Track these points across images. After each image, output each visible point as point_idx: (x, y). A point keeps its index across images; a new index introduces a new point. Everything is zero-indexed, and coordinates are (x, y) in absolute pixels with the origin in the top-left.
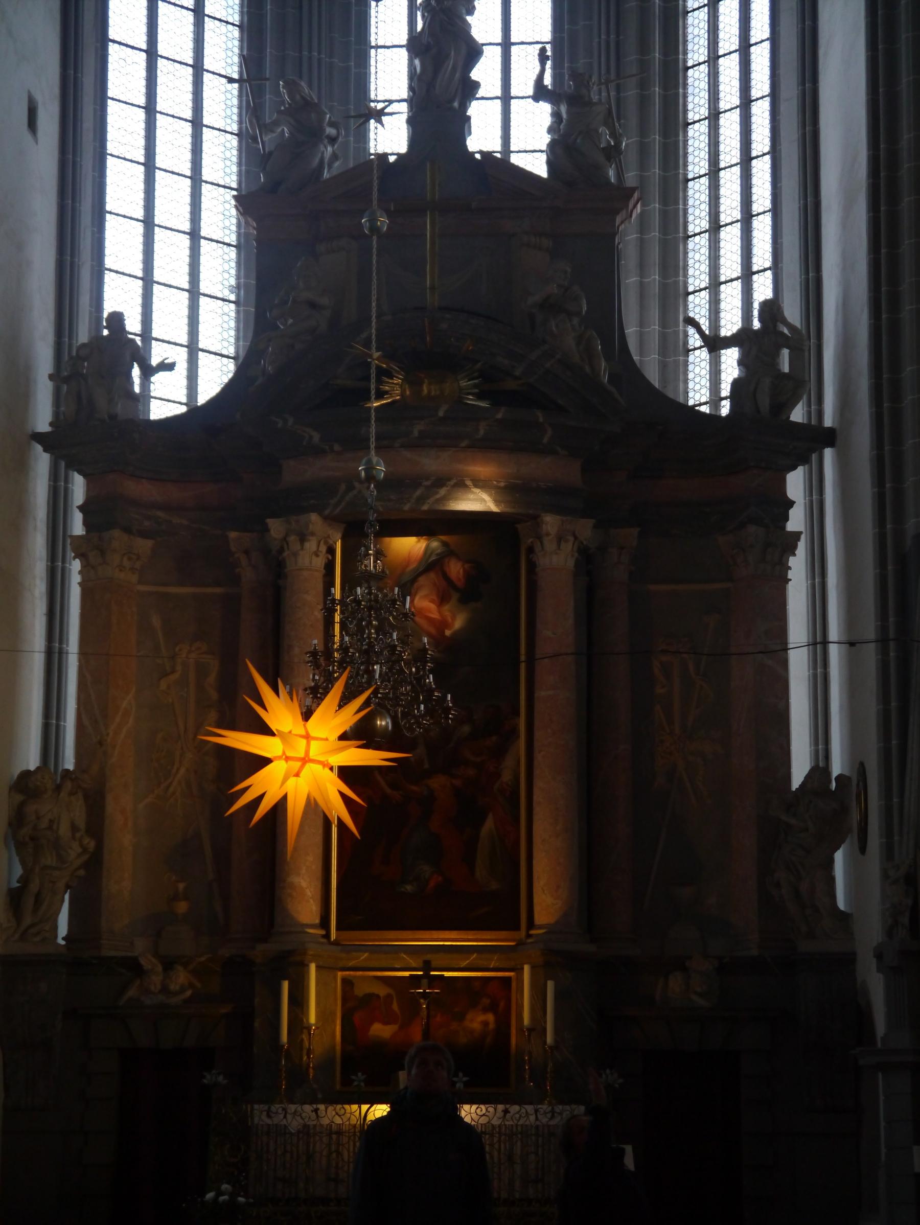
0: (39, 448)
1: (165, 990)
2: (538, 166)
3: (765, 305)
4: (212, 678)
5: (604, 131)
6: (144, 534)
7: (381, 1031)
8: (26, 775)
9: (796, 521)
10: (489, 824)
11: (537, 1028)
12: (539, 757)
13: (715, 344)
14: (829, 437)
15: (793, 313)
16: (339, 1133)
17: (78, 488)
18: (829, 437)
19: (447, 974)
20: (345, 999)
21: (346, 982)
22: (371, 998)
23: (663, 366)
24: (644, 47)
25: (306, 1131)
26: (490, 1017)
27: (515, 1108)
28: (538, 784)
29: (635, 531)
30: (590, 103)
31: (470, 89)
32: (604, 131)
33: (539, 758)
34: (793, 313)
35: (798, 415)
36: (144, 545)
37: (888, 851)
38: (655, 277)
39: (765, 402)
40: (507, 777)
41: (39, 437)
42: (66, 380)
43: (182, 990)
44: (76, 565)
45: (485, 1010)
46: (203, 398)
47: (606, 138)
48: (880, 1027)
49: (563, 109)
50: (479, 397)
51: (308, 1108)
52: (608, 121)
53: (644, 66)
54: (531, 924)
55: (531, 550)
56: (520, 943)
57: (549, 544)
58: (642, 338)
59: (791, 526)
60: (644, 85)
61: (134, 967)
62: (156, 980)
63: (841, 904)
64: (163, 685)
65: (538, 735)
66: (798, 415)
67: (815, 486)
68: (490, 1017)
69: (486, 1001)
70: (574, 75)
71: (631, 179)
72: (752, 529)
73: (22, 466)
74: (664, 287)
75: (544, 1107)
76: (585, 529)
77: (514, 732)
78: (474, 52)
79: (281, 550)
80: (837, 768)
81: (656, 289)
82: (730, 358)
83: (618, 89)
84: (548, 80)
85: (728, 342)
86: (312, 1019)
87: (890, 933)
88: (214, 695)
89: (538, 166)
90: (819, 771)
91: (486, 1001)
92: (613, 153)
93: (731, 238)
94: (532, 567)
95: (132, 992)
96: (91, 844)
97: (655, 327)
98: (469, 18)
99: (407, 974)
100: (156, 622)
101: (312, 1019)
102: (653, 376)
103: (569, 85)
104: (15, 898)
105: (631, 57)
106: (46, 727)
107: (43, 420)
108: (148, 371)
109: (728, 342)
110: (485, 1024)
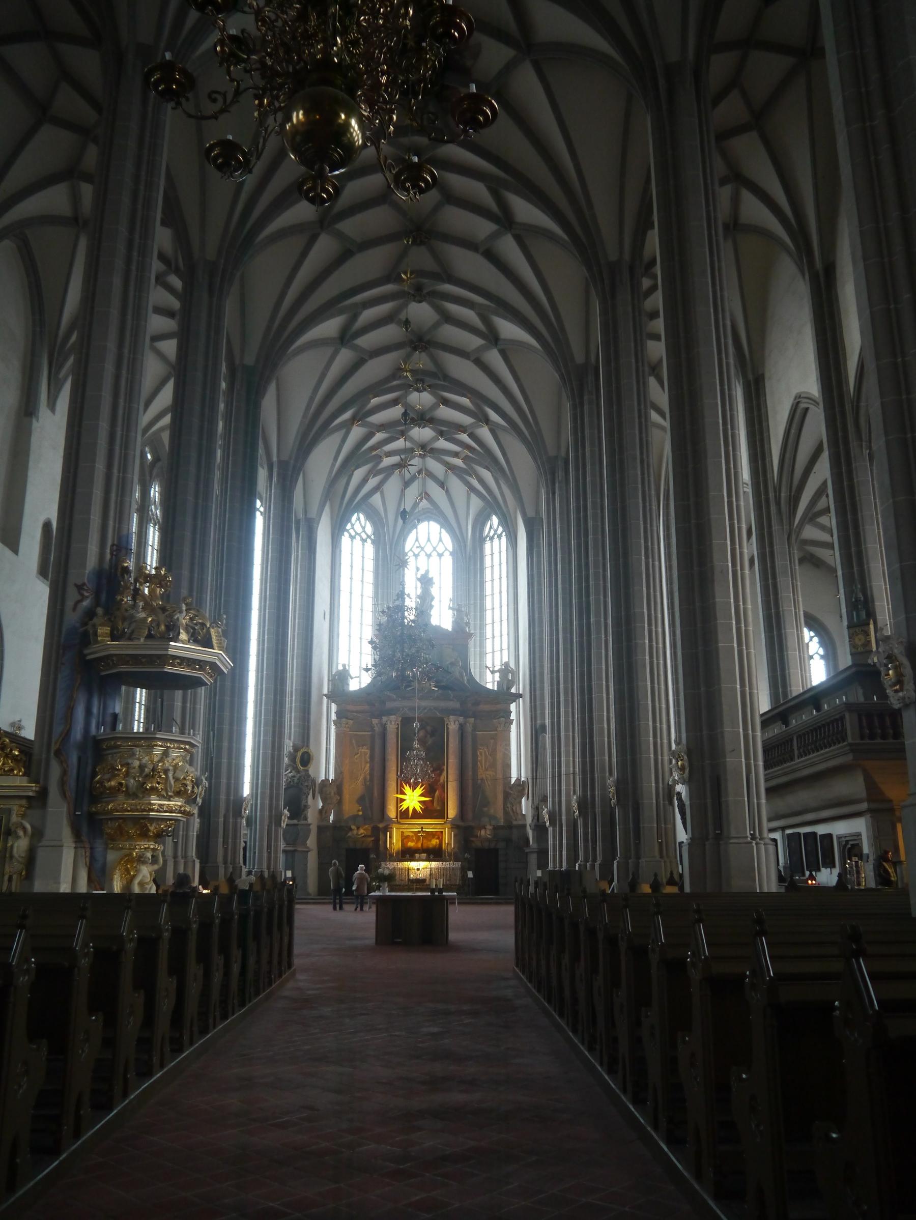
0: (325, 698)
1: (357, 834)
2: (450, 629)
3: (505, 662)
4: (368, 755)
5: (465, 618)
6: (352, 720)
7: (411, 844)
8: (322, 780)
9: (513, 716)
10: (437, 793)
11: (449, 844)
12: (450, 776)
13: (493, 672)
14: (520, 696)
15: (512, 665)
16: (402, 869)
17: (334, 707)
18: (520, 696)
19: (427, 830)
20: (402, 837)
21: (402, 832)
22: (408, 836)
23: (480, 677)
24: (475, 590)
25: (394, 869)
26: (438, 841)
27: (444, 863)
28: (449, 783)
29: (473, 719)
30: (462, 611)
31: (431, 607)
32: (465, 618)
33: (449, 776)
34: (512, 665)
35: (513, 690)
36: (351, 722)
37: (533, 800)
38: (478, 649)
39: (505, 688)
40: (441, 781)
41: (325, 695)
42: (331, 681)
43: (362, 834)
44: (333, 727)
45: (436, 839)
46: (364, 685)
47: (466, 620)
48: (531, 843)
49: (455, 613)
50: (435, 687)
51: (396, 863)
52: (466, 615)
53: (475, 596)
54: (447, 818)
55: (447, 724)
56: (445, 823)
57: (452, 723)
58: (475, 672)
59: (512, 718)
60: (475, 599)
61: (351, 829)
62: (355, 832)
63: (523, 813)
64: (356, 757)
65: (449, 771)
66: (513, 690)
67: (518, 707)
68: (438, 841)
69: (436, 837)
70: (458, 605)
71: (472, 631)
72: (502, 719)
73: (320, 703)
74: (480, 651)
75: (451, 862)
76: (461, 719)
77: (443, 770)
78: (433, 598)
79: (386, 724)
80: (523, 779)
81: (478, 652)
82: (497, 675)
83: (469, 607)
84: (451, 606)
85: (496, 672)
86: (395, 842)
87: (532, 820)
88: (369, 760)
89: (450, 629)
90: (518, 780)
91: (436, 837)
92: (467, 624)
93: (497, 640)
94: (448, 728)
95: (350, 834)
96: (339, 798)
97: (478, 662)
98: (431, 589)
99: (417, 830)
100: (354, 741)
101: (395, 842)
102: (478, 681)
103: (456, 606)
104: (321, 811)
105: (472, 593)
106: (326, 767)
107: (325, 692)
108: (352, 678)
109: (496, 672)
110: (436, 842)
